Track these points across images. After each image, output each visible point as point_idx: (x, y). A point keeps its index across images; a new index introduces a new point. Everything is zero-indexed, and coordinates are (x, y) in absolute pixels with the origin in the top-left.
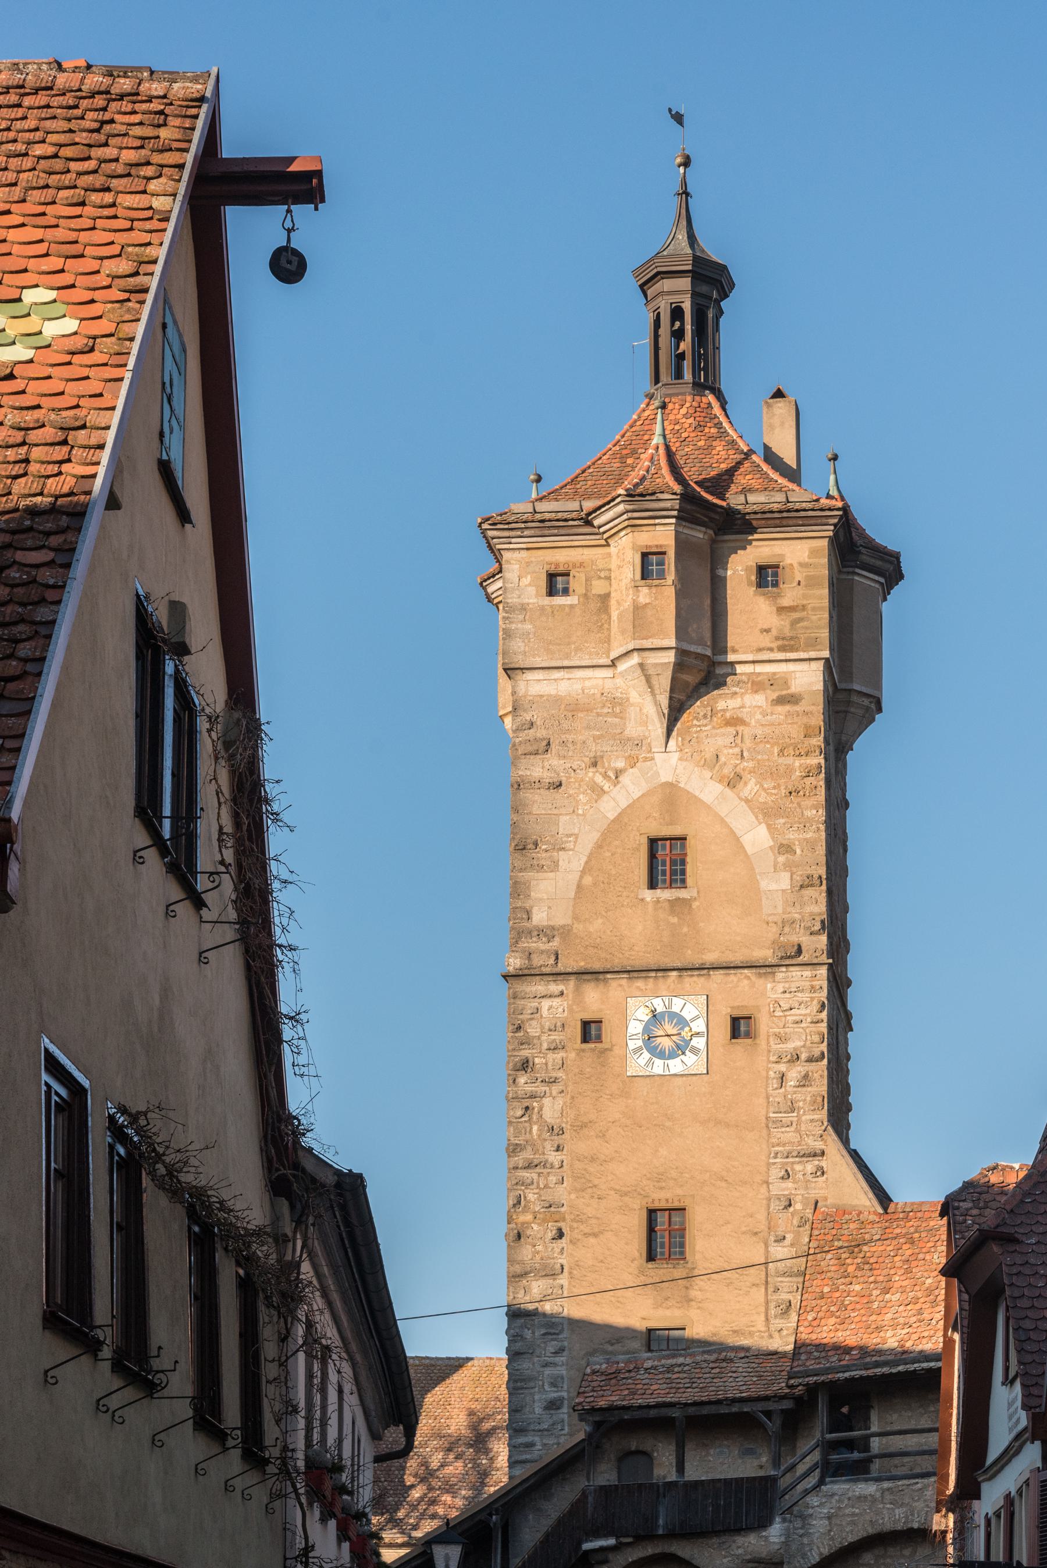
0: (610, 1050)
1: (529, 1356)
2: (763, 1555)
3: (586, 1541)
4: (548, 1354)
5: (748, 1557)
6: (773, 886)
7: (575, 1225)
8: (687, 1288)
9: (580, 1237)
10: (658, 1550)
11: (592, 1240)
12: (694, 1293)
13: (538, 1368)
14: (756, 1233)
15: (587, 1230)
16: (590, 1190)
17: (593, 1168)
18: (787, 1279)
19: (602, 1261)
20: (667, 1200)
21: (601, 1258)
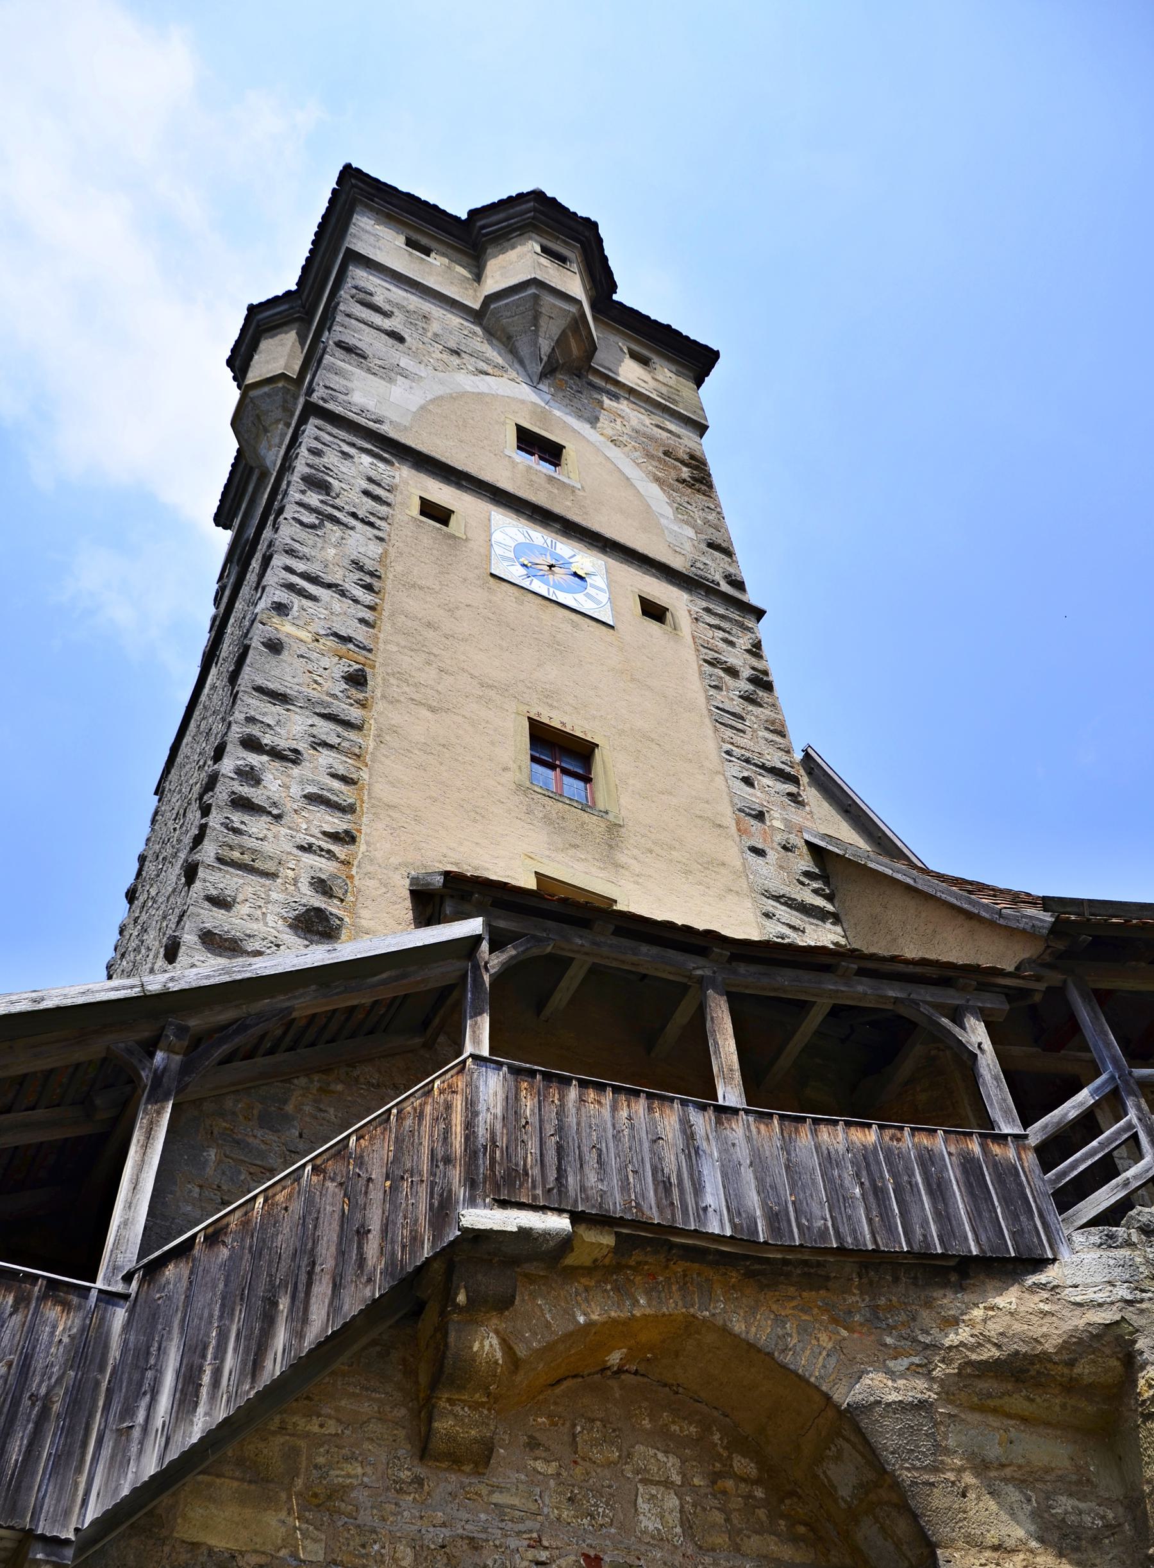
0: (467, 540)
1: (269, 819)
2: (1049, 1346)
3: (472, 1202)
4: (316, 832)
5: (989, 1353)
6: (676, 528)
7: (393, 681)
8: (610, 846)
9: (402, 699)
10: (673, 1306)
11: (425, 713)
12: (622, 858)
13: (289, 847)
14: (720, 826)
15: (416, 696)
16: (424, 656)
17: (430, 634)
18: (784, 908)
19: (444, 746)
20: (564, 724)
21: (443, 742)
